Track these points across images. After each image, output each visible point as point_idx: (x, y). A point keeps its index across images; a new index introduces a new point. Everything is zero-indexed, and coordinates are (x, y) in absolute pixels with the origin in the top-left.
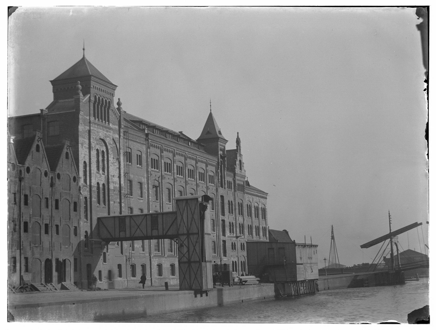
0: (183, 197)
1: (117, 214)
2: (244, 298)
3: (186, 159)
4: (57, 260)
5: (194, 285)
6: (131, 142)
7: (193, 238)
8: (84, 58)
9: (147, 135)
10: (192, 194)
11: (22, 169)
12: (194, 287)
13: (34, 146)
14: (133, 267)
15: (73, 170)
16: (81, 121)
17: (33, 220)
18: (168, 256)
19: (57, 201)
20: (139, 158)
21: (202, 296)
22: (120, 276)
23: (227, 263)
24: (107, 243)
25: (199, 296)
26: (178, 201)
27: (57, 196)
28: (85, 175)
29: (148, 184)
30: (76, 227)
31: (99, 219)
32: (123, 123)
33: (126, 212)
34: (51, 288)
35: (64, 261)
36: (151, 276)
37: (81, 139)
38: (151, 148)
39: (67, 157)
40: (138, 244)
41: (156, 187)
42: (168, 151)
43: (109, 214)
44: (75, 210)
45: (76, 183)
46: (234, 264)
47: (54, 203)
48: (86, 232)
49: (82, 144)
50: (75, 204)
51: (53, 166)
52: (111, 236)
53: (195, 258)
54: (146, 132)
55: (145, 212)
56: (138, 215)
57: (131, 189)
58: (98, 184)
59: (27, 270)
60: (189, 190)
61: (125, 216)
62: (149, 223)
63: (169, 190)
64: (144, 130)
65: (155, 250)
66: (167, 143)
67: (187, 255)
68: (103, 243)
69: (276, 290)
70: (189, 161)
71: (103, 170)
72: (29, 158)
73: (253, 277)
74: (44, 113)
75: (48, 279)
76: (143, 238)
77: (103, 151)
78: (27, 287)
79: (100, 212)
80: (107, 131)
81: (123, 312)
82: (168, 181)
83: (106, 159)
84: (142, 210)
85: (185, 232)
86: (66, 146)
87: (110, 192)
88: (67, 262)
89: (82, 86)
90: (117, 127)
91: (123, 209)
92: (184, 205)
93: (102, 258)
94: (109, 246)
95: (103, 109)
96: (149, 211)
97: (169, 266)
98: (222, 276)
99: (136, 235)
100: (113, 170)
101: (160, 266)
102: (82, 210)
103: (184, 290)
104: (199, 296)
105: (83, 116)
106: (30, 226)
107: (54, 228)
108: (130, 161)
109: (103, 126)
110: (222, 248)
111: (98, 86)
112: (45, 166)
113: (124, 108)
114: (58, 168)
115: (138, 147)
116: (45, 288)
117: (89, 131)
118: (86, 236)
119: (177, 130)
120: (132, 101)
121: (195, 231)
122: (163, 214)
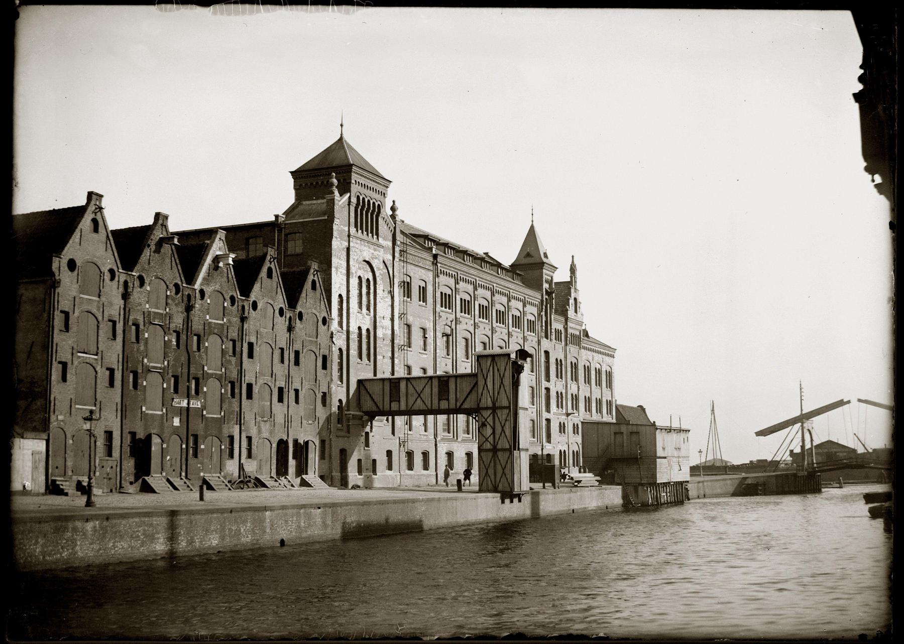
0: (488, 352)
1: (388, 375)
2: (575, 507)
3: (493, 295)
4: (296, 442)
5: (500, 485)
6: (410, 267)
7: (502, 414)
8: (341, 139)
9: (435, 257)
10: (501, 348)
11: (246, 304)
12: (500, 488)
13: (264, 271)
14: (410, 455)
15: (323, 306)
16: (335, 233)
17: (261, 381)
18: (463, 441)
19: (297, 353)
20: (423, 290)
21: (512, 502)
22: (390, 468)
23: (551, 453)
24: (372, 419)
25: (507, 501)
26: (480, 357)
27: (297, 346)
28: (341, 315)
29: (435, 330)
30: (325, 394)
31: (360, 382)
32: (399, 237)
33: (400, 373)
34: (286, 483)
35: (307, 443)
36: (436, 470)
37: (335, 261)
38: (441, 276)
39: (314, 287)
40: (417, 420)
41: (448, 336)
42: (466, 281)
43: (375, 375)
44: (324, 367)
45: (326, 327)
46: (563, 454)
47: (292, 356)
48: (340, 401)
49: (337, 268)
50: (325, 358)
51: (293, 300)
52: (378, 407)
53: (504, 444)
54: (434, 252)
55: (430, 373)
56: (420, 378)
57: (409, 338)
58: (360, 328)
59: (250, 456)
60: (497, 342)
61: (399, 379)
62: (436, 390)
63: (467, 340)
64: (431, 249)
65: (444, 430)
66: (465, 269)
67: (491, 439)
68: (366, 418)
69: (625, 497)
70: (497, 297)
71: (368, 309)
72: (257, 287)
73: (591, 475)
74: (281, 220)
75: (282, 470)
76: (425, 413)
77: (368, 280)
78: (249, 481)
79: (361, 371)
80: (375, 250)
81: (387, 520)
82: (465, 327)
83: (372, 291)
84: (425, 370)
85: (490, 404)
86: (312, 271)
87: (378, 342)
88: (310, 444)
89: (338, 181)
90: (390, 244)
91: (396, 368)
92: (489, 364)
93: (363, 439)
94: (374, 422)
95: (368, 216)
96: (435, 370)
97: (464, 455)
98: (543, 470)
99: (415, 407)
100: (383, 308)
101: (450, 455)
102: (335, 367)
103: (485, 492)
104: (507, 501)
105: (340, 226)
106: (256, 390)
107: (292, 394)
108: (409, 296)
109: (368, 242)
110: (544, 430)
111: (363, 181)
112: (280, 301)
113: (400, 215)
114: (300, 303)
115: (420, 275)
116: (277, 484)
117: (348, 249)
118: (340, 408)
119: (480, 251)
120: (415, 205)
121: (505, 403)
122: (457, 377)
